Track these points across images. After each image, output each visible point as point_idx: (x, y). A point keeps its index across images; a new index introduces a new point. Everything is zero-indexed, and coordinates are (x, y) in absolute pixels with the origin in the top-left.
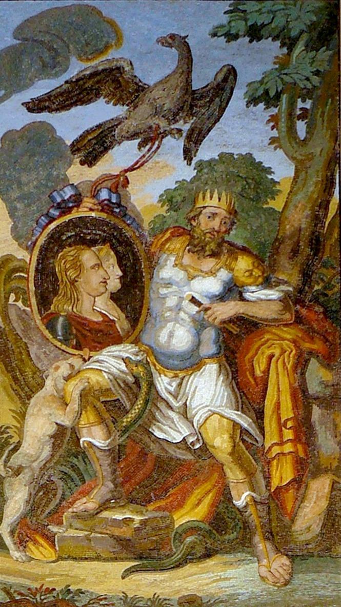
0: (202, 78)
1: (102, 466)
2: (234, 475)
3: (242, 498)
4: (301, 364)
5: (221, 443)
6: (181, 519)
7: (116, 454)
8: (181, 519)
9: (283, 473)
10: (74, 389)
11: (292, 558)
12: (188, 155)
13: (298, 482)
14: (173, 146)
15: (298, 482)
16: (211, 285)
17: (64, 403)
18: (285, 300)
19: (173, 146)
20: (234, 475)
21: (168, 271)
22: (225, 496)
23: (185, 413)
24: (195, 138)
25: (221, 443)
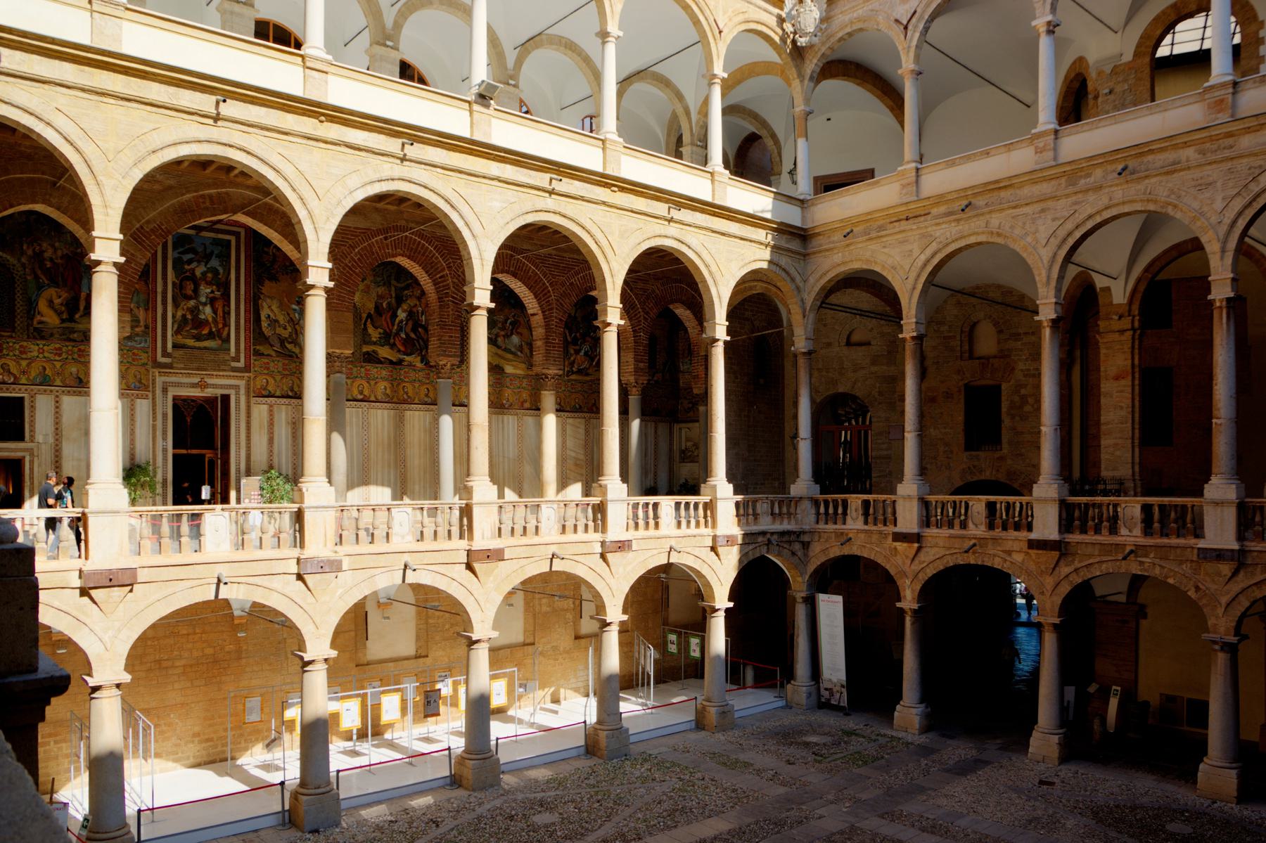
0: (208, 251)
1: (190, 322)
2: (213, 326)
3: (214, 330)
4: (224, 306)
5: (210, 319)
6: (204, 332)
7: (192, 320)
8: (204, 332)
9: (220, 326)
10: (185, 307)
11: (223, 341)
12: (206, 266)
13: (223, 327)
14: (203, 264)
15: (223, 327)
16: (209, 290)
17: (183, 309)
18: (221, 295)
19: (203, 264)
20: (213, 326)
21: (202, 287)
22: (211, 329)
23: (204, 314)
24: (206, 264)
25: (210, 319)
